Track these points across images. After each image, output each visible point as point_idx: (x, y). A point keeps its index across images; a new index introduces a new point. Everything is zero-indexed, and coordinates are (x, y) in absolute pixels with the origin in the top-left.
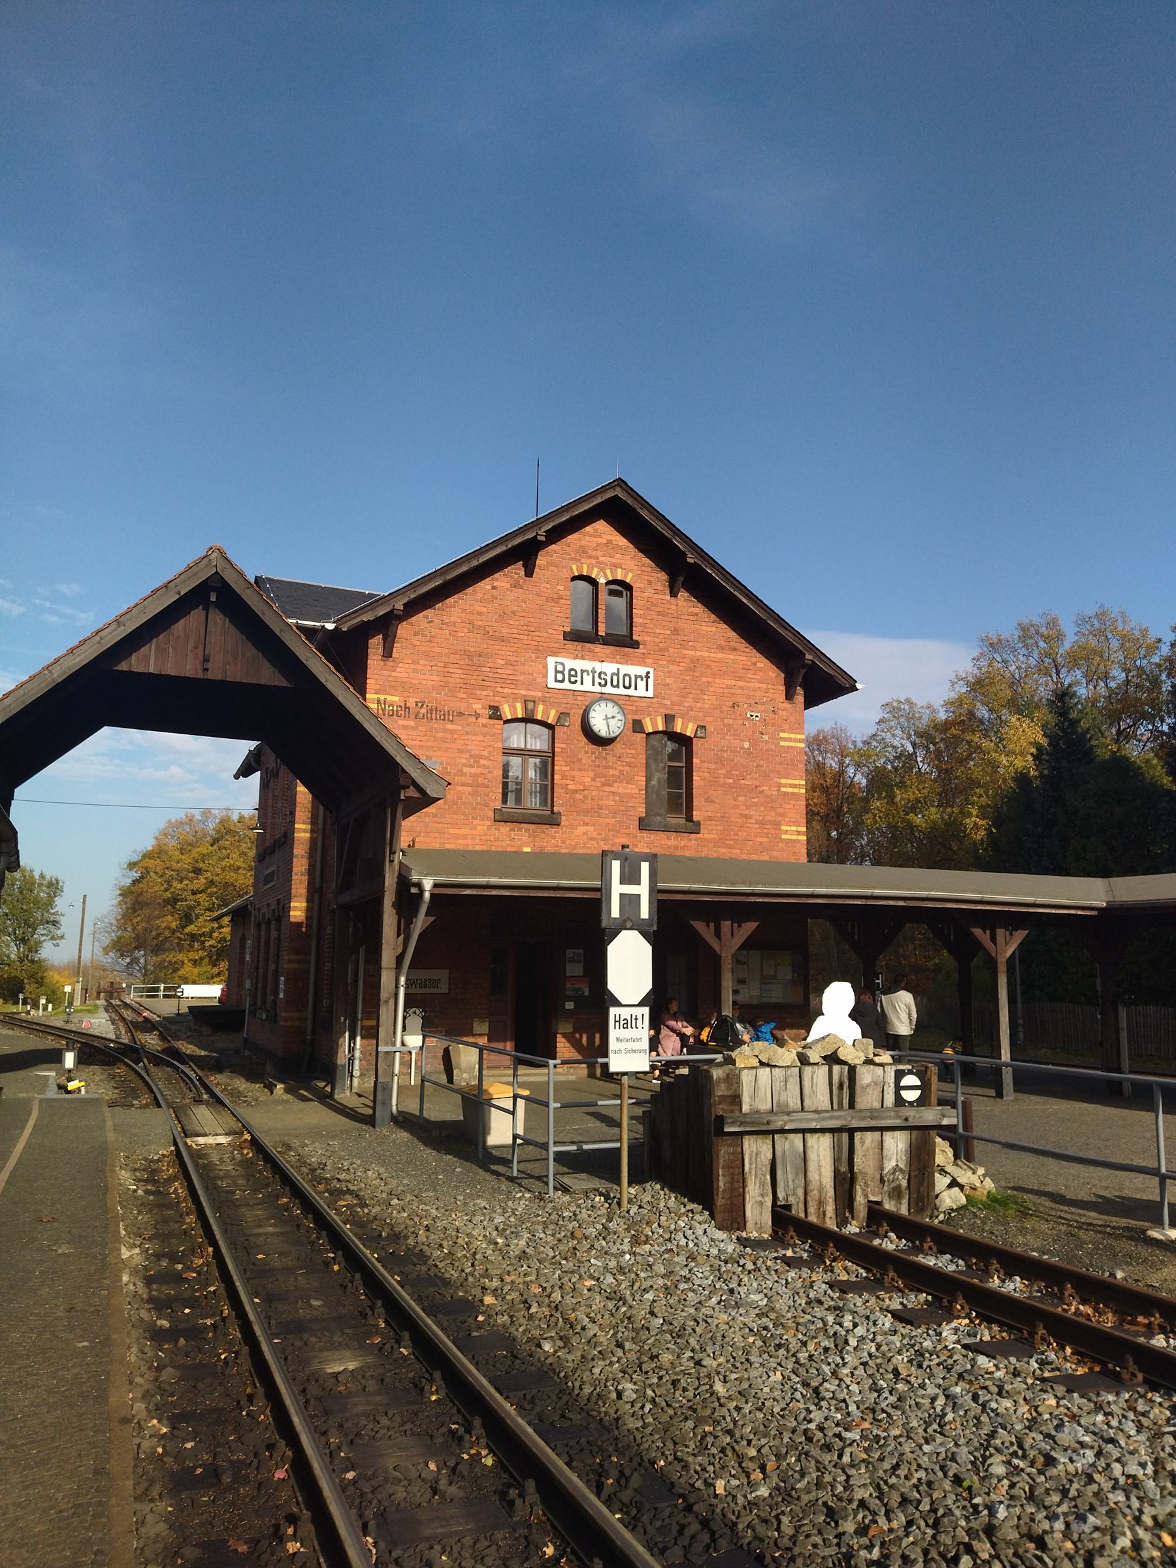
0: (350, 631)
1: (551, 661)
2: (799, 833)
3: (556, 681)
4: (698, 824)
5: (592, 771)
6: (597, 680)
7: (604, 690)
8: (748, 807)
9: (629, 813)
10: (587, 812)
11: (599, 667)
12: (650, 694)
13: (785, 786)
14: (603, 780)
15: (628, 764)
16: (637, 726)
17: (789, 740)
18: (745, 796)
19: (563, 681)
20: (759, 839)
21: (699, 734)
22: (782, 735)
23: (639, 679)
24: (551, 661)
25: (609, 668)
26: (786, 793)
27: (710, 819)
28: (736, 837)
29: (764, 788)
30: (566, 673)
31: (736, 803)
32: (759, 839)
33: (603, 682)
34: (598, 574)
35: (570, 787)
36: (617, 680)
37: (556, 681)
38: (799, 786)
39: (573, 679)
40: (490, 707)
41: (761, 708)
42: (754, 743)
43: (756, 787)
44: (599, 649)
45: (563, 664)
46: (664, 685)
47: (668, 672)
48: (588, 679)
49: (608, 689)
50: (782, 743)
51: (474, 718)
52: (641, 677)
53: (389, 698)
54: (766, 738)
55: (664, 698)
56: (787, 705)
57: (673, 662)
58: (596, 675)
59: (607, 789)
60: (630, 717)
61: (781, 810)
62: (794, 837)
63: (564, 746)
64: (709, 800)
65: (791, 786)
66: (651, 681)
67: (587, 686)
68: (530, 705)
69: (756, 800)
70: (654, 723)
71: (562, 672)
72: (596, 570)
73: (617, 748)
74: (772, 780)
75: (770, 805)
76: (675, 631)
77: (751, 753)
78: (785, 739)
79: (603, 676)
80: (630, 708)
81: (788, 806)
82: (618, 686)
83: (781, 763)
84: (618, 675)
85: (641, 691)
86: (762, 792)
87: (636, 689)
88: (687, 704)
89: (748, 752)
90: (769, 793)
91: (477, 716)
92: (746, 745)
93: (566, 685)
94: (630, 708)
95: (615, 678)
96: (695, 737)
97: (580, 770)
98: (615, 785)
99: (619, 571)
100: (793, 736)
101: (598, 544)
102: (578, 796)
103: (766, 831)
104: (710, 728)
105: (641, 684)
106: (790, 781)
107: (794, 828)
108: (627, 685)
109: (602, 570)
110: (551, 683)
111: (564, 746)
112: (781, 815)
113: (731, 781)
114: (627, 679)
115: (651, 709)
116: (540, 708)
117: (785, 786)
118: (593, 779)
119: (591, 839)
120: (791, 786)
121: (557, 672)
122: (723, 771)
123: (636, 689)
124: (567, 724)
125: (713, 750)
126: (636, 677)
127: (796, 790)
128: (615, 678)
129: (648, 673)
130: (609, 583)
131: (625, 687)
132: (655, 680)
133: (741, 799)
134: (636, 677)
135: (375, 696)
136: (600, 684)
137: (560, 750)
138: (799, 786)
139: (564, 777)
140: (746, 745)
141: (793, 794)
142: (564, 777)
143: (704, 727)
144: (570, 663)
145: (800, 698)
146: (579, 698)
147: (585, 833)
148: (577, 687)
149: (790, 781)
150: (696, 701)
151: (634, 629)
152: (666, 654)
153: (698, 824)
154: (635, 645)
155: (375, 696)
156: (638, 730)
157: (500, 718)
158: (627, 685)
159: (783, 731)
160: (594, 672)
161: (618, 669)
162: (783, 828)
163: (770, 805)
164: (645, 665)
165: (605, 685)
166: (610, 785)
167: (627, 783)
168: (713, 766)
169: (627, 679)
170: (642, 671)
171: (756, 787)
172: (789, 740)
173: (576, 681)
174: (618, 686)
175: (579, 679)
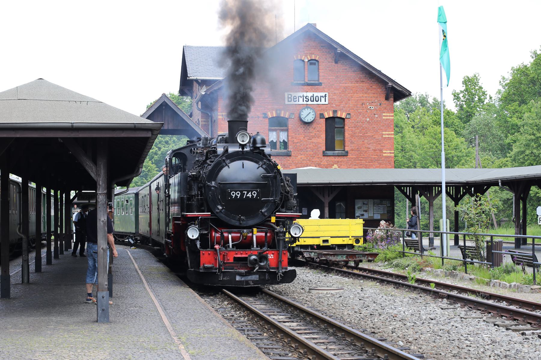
3: (288, 101)
4: (347, 152)
5: (304, 134)
6: (305, 99)
7: (308, 103)
8: (369, 144)
9: (318, 150)
10: (301, 150)
11: (305, 94)
12: (327, 103)
13: (385, 135)
14: (308, 137)
15: (318, 131)
16: (322, 116)
17: (387, 116)
18: (368, 139)
19: (291, 101)
20: (373, 156)
21: (347, 117)
22: (384, 114)
23: (322, 98)
25: (310, 94)
26: (386, 138)
28: (363, 156)
29: (376, 136)
30: (292, 98)
31: (363, 143)
32: (373, 156)
34: (304, 58)
35: (295, 141)
37: (288, 101)
39: (295, 100)
40: (264, 114)
41: (374, 104)
42: (372, 119)
43: (372, 136)
45: (291, 95)
46: (333, 99)
47: (334, 93)
49: (310, 102)
50: (384, 118)
51: (257, 118)
52: (323, 97)
54: (376, 116)
55: (332, 104)
56: (387, 102)
58: (304, 98)
59: (309, 141)
60: (319, 113)
61: (383, 145)
62: (389, 155)
63: (292, 126)
64: (352, 143)
65: (388, 135)
66: (327, 98)
67: (301, 102)
68: (278, 112)
69: (372, 141)
71: (291, 98)
72: (304, 57)
73: (314, 125)
74: (379, 133)
75: (378, 143)
77: (370, 123)
78: (385, 116)
80: (319, 109)
81: (386, 143)
82: (313, 101)
83: (383, 126)
84: (313, 96)
85: (323, 102)
86: (374, 138)
87: (321, 101)
88: (342, 105)
89: (369, 122)
90: (378, 138)
91: (259, 117)
92: (368, 120)
93: (293, 103)
94: (319, 109)
95: (312, 98)
96: (346, 118)
97: (299, 134)
98: (313, 139)
99: (313, 56)
100: (388, 114)
102: (298, 144)
103: (376, 153)
104: (352, 114)
105: (323, 99)
106: (387, 133)
107: (389, 151)
108: (317, 100)
109: (306, 56)
110: (287, 103)
111: (292, 126)
112: (382, 146)
113: (361, 134)
114: (317, 98)
115: (327, 109)
116: (283, 112)
117: (385, 135)
118: (304, 138)
119: (304, 160)
120: (388, 135)
121: (288, 98)
123: (321, 101)
124: (293, 117)
125: (354, 123)
126: (321, 97)
128: (312, 98)
129: (326, 94)
130: (309, 61)
131: (316, 101)
132: (329, 97)
133: (366, 141)
135: (221, 114)
136: (306, 101)
137: (290, 127)
139: (292, 138)
141: (388, 138)
142: (292, 138)
143: (350, 114)
145: (392, 99)
146: (298, 107)
147: (301, 158)
148: (297, 103)
149: (387, 133)
150: (346, 104)
151: (320, 78)
153: (347, 152)
154: (320, 84)
155: (221, 114)
156: (322, 117)
157: (267, 117)
158: (317, 100)
159: (384, 113)
160: (303, 96)
161: (313, 95)
162: (384, 151)
163: (378, 143)
164: (324, 92)
165: (308, 101)
166: (311, 139)
167: (318, 138)
168: (353, 129)
169: (317, 98)
171: (372, 136)
172: (387, 116)
173: (296, 101)
174: (313, 101)
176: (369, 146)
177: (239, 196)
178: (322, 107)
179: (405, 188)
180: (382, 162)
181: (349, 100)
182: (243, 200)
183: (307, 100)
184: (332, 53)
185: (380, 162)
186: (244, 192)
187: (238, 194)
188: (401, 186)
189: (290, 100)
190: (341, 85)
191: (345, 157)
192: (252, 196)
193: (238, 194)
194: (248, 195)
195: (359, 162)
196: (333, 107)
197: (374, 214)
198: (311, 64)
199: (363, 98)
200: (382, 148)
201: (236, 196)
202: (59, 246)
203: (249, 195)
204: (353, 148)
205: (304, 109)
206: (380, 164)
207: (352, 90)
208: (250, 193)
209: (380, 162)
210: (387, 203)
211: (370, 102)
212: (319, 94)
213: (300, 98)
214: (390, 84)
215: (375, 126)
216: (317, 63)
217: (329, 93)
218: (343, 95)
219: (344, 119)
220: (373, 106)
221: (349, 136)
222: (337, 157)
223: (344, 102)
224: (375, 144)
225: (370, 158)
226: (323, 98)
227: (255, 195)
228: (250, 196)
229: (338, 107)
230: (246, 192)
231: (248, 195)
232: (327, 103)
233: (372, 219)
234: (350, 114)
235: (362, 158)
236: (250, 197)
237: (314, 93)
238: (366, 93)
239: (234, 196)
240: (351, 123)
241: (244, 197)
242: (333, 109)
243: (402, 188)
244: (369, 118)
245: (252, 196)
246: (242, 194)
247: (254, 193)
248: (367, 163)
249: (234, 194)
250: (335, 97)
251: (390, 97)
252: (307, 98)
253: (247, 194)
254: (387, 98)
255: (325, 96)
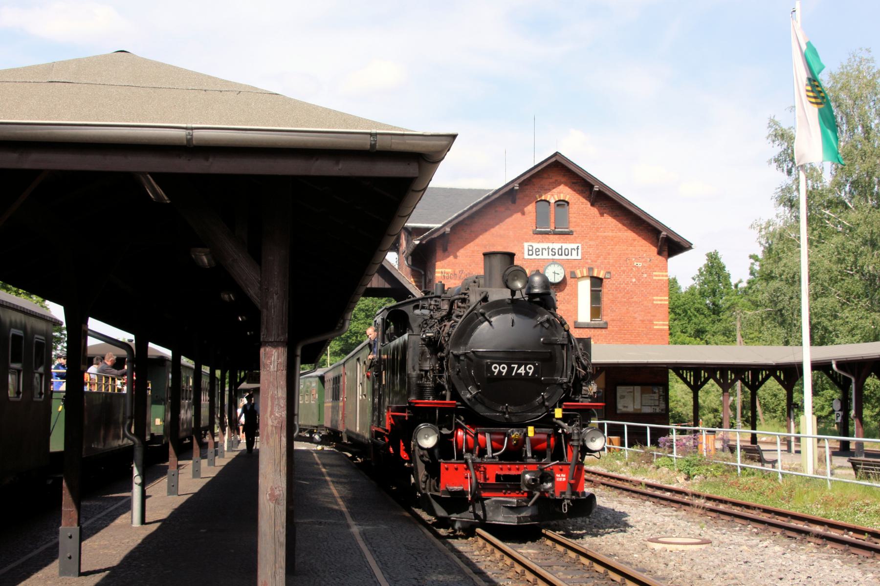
0: (427, 242)
1: (526, 245)
2: (664, 325)
3: (529, 255)
11: (551, 246)
12: (579, 257)
13: (657, 300)
17: (659, 276)
18: (633, 307)
19: (532, 255)
20: (641, 329)
21: (607, 276)
22: (654, 273)
23: (573, 251)
24: (526, 245)
25: (557, 246)
26: (657, 304)
27: (613, 320)
32: (641, 329)
33: (554, 253)
36: (561, 252)
37: (529, 255)
38: (665, 300)
39: (537, 253)
42: (639, 280)
44: (551, 237)
46: (587, 252)
48: (545, 252)
49: (557, 257)
50: (654, 278)
53: (447, 270)
54: (645, 275)
55: (587, 259)
57: (591, 240)
58: (550, 250)
60: (569, 270)
65: (661, 300)
66: (580, 251)
67: (545, 256)
69: (640, 309)
70: (582, 272)
71: (532, 250)
76: (593, 223)
78: (656, 276)
79: (554, 250)
82: (562, 255)
84: (561, 249)
85: (574, 256)
86: (642, 305)
87: (571, 255)
89: (635, 284)
92: (634, 280)
93: (534, 257)
95: (560, 251)
96: (605, 278)
100: (661, 273)
101: (550, 183)
104: (613, 273)
105: (574, 253)
106: (659, 298)
108: (567, 254)
110: (526, 256)
113: (625, 300)
114: (566, 251)
117: (657, 300)
120: (661, 300)
121: (529, 250)
122: (621, 294)
123: (571, 255)
125: (615, 284)
126: (572, 249)
127: (663, 302)
128: (560, 251)
131: (565, 255)
133: (631, 309)
134: (572, 249)
138: (665, 300)
140: (634, 280)
141: (661, 304)
143: (609, 273)
144: (536, 245)
145: (666, 253)
148: (540, 257)
149: (659, 298)
150: (605, 259)
152: (588, 235)
156: (573, 276)
158: (567, 254)
159: (655, 271)
160: (548, 248)
162: (655, 323)
164: (576, 243)
165: (555, 255)
169: (566, 251)
170: (575, 246)
172: (659, 276)
174: (562, 255)
175: (540, 253)
176: (636, 315)
177: (505, 371)
178: (573, 263)
179: (685, 371)
180: (652, 336)
181: (609, 254)
182: (509, 379)
183: (554, 253)
184: (586, 193)
185: (650, 336)
186: (512, 366)
187: (504, 368)
188: (678, 368)
189: (531, 253)
190: (598, 233)
191: (603, 330)
192: (527, 373)
193: (504, 368)
194: (519, 371)
195: (622, 336)
196: (587, 263)
197: (642, 405)
198: (558, 205)
199: (627, 252)
200: (652, 318)
201: (500, 372)
202: (110, 495)
203: (522, 371)
204: (615, 318)
205: (550, 265)
206: (650, 339)
207: (612, 240)
208: (523, 367)
209: (650, 336)
210: (658, 390)
211: (637, 256)
212: (570, 246)
213: (544, 250)
214: (664, 233)
215: (642, 289)
216: (566, 204)
217: (582, 245)
218: (601, 247)
219: (601, 280)
220: (641, 262)
221: (609, 301)
222: (592, 330)
223: (601, 257)
224: (643, 313)
225: (636, 331)
226: (575, 250)
227: (531, 372)
228: (523, 372)
229: (594, 263)
230: (516, 366)
231: (519, 371)
232: (580, 258)
233: (639, 412)
234: (609, 273)
235: (626, 331)
236: (523, 374)
237: (563, 244)
238: (631, 245)
239: (496, 371)
240: (611, 284)
241: (513, 374)
242: (587, 266)
243: (681, 371)
244: (635, 278)
245: (527, 373)
246: (510, 370)
247: (530, 368)
248: (632, 338)
249: (496, 369)
250: (591, 250)
251: (664, 251)
252: (554, 250)
253: (518, 369)
254: (659, 253)
255: (578, 249)
